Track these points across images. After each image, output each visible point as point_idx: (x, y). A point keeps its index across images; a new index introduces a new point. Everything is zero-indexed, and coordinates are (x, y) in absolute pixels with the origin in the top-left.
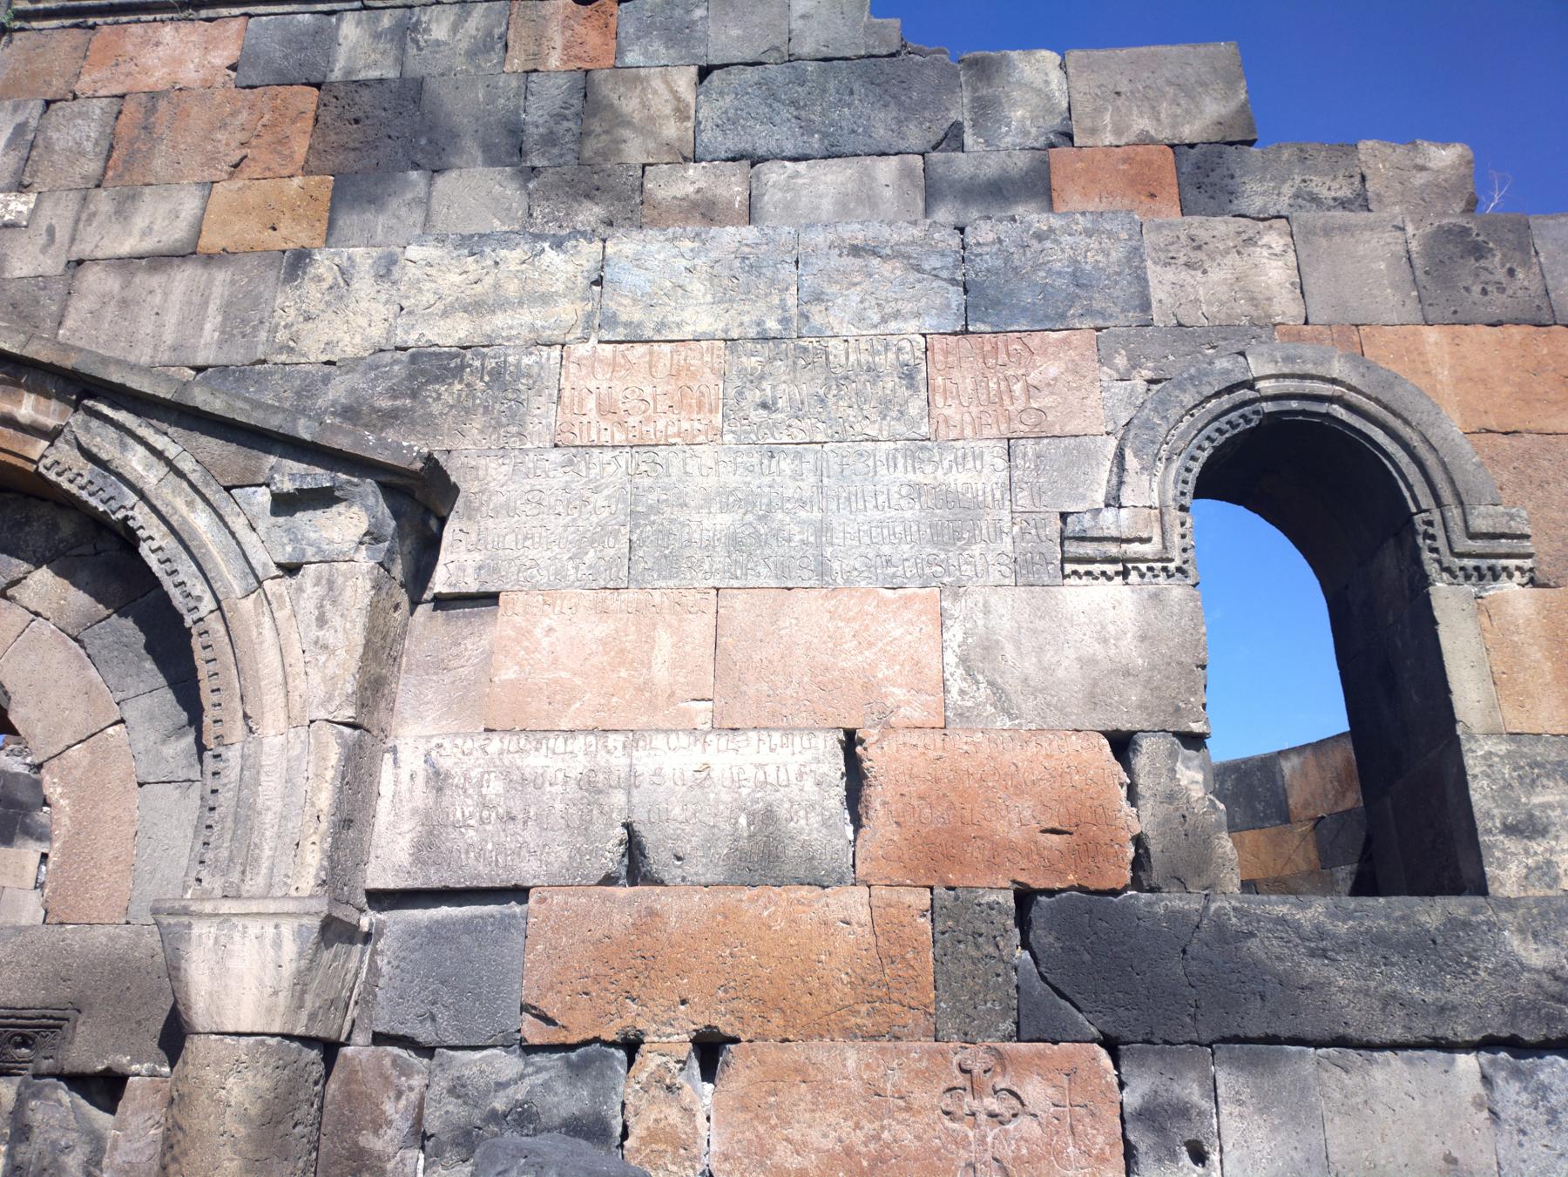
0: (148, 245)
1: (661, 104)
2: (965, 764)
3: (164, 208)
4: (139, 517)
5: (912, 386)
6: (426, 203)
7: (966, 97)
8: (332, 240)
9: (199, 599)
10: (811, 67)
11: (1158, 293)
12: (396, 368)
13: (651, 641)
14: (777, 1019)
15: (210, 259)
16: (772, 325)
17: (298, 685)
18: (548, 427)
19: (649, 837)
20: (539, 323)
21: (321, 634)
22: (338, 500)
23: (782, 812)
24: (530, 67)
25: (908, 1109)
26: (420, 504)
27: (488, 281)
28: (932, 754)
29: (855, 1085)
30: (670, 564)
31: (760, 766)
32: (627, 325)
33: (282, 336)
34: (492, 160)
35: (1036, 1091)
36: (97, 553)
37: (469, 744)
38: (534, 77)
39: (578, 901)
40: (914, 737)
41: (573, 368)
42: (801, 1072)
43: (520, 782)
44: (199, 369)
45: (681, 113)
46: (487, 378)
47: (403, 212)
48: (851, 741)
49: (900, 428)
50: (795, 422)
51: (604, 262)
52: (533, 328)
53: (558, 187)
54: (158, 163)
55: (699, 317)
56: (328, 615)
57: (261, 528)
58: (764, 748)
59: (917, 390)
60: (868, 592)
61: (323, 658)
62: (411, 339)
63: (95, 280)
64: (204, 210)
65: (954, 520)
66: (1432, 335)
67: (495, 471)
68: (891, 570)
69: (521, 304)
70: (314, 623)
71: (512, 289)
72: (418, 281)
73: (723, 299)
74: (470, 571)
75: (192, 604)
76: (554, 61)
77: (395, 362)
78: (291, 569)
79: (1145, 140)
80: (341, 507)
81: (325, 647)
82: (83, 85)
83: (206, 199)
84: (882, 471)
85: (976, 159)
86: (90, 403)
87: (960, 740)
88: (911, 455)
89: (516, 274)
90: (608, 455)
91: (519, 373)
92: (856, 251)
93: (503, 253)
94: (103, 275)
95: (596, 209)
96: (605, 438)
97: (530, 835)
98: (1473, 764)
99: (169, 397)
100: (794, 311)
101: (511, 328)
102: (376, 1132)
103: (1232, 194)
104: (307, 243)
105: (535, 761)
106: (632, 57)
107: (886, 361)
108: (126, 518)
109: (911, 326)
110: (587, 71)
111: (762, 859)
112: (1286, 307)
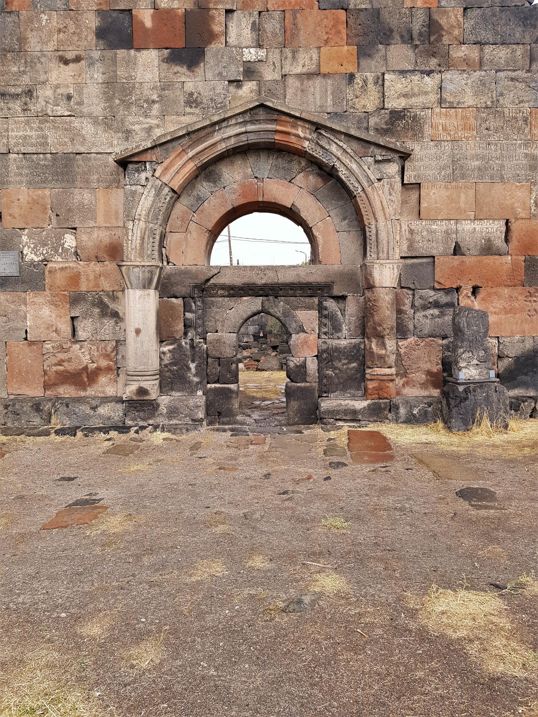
0: (305, 70)
2: (534, 227)
5: (526, 124)
8: (359, 70)
9: (357, 188)
10: (498, 9)
13: (459, 196)
14: (490, 283)
16: (489, 103)
17: (387, 211)
18: (429, 135)
19: (462, 245)
20: (425, 101)
22: (391, 161)
23: (492, 239)
24: (412, 6)
25: (517, 300)
27: (409, 86)
28: (527, 225)
29: (507, 296)
30: (463, 176)
31: (487, 228)
32: (449, 102)
34: (404, 42)
38: (413, 10)
39: (446, 259)
40: (523, 221)
41: (435, 116)
42: (495, 293)
43: (431, 232)
44: (328, 113)
47: (379, 60)
49: (523, 137)
50: (495, 134)
52: (423, 104)
53: (424, 52)
54: (301, 38)
55: (469, 100)
57: (371, 169)
58: (488, 224)
59: (527, 125)
60: (513, 184)
64: (319, 57)
68: (519, 178)
71: (416, 89)
75: (356, 189)
77: (386, 113)
78: (379, 180)
80: (392, 164)
82: (270, 6)
83: (319, 53)
84: (518, 149)
86: (320, 131)
88: (525, 145)
90: (446, 143)
92: (512, 79)
93: (413, 77)
96: (445, 138)
97: (434, 244)
100: (495, 99)
105: (433, 227)
108: (334, 165)
109: (527, 105)
110: (429, 8)
111: (488, 249)
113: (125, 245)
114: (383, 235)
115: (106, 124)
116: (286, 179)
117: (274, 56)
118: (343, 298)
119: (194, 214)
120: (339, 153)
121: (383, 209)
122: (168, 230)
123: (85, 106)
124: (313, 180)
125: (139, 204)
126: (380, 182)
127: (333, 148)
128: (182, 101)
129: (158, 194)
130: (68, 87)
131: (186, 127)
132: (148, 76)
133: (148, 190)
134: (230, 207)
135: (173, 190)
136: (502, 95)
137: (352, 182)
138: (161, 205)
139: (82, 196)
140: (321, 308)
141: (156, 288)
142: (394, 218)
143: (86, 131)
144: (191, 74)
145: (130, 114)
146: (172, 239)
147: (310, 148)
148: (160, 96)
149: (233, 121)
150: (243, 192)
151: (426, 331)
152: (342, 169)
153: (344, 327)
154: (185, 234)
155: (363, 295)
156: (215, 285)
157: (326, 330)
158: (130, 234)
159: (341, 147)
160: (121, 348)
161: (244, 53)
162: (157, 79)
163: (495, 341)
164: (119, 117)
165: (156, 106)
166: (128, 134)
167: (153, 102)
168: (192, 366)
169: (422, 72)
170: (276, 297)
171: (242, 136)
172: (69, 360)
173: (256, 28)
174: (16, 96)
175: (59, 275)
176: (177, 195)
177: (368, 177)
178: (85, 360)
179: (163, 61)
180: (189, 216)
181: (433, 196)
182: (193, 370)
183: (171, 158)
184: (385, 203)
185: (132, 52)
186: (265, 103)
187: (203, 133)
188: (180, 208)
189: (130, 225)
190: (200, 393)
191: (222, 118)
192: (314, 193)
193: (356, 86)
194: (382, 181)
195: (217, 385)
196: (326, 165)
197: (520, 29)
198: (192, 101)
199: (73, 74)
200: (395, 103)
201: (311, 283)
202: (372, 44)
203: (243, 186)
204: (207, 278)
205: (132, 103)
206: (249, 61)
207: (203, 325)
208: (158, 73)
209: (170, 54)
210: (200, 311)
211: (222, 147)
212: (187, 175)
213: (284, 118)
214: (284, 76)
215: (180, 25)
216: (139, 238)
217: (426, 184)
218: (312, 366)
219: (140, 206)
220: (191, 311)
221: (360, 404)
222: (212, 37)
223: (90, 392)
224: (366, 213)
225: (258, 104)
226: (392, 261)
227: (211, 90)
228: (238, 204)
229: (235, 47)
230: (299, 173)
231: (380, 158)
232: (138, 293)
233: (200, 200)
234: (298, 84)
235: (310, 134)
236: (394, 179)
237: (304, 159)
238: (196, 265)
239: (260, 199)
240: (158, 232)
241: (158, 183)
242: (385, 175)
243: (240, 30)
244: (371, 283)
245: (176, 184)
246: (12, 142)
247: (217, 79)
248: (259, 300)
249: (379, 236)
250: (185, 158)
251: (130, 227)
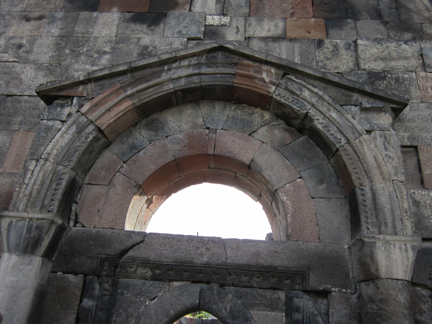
0: (270, 34)
3: (272, 24)
4: (312, 113)
9: (340, 139)
12: (364, 75)
15: (291, 40)
20: (406, 65)
21: (387, 153)
27: (386, 52)
33: (321, 64)
36: (279, 125)
37: (423, 193)
46: (394, 80)
47: (349, 31)
51: (421, 49)
52: (404, 67)
56: (388, 147)
57: (357, 118)
61: (390, 161)
62: (367, 67)
64: (286, 25)
69: (399, 59)
70: (384, 149)
71: (394, 54)
72: (364, 50)
74: (406, 139)
75: (338, 141)
77: (362, 74)
78: (369, 132)
80: (383, 114)
81: (390, 157)
83: (285, 22)
86: (289, 76)
89: (395, 51)
93: (389, 44)
94: (258, 42)
95: (409, 34)
99: (320, 76)
101: (398, 66)
102: (421, 314)
104: (321, 37)
108: (307, 113)
113: (17, 189)
114: (384, 200)
115: (48, 70)
116: (244, 132)
118: (325, 294)
119: (125, 165)
121: (379, 166)
122: (86, 181)
123: (32, 54)
124: (279, 133)
125: (51, 142)
126: (371, 135)
127: (306, 94)
128: (136, 53)
129: (79, 131)
130: (22, 38)
131: (130, 63)
132: (105, 32)
133: (67, 126)
134: (170, 158)
135: (99, 129)
137: (332, 132)
138: (79, 144)
141: (47, 255)
142: (396, 178)
143: (26, 75)
144: (149, 32)
145: (77, 62)
146: (89, 193)
147: (277, 93)
148: (112, 48)
149: (185, 63)
150: (189, 143)
152: (319, 117)
154: (107, 188)
155: (355, 292)
156: (134, 259)
158: (29, 176)
159: (316, 93)
161: (207, 19)
162: (114, 35)
164: (64, 63)
165: (107, 56)
167: (105, 53)
170: (222, 286)
171: (194, 78)
177: (353, 127)
179: (124, 21)
180: (117, 167)
183: (105, 94)
184: (380, 158)
185: (95, 14)
186: (224, 45)
187: (148, 71)
188: (108, 156)
189: (32, 165)
191: (172, 56)
192: (280, 148)
193: (325, 50)
194: (373, 134)
196: (296, 115)
199: (31, 29)
201: (275, 268)
204: (123, 247)
205: (82, 53)
206: (212, 25)
208: (116, 30)
209: (133, 16)
210: (107, 297)
212: (121, 114)
213: (246, 62)
216: (38, 183)
217: (425, 148)
219: (52, 144)
220: (92, 297)
224: (355, 171)
225: (216, 45)
226: (404, 238)
227: (168, 45)
228: (181, 156)
230: (262, 126)
231: (368, 106)
232: (14, 258)
233: (135, 149)
234: (262, 45)
235: (277, 79)
236: (388, 132)
237: (267, 112)
238: (112, 229)
239: (211, 152)
241: (83, 119)
242: (375, 127)
244: (373, 270)
247: (176, 36)
248: (197, 288)
249: (378, 201)
250: (123, 96)
251: (32, 168)
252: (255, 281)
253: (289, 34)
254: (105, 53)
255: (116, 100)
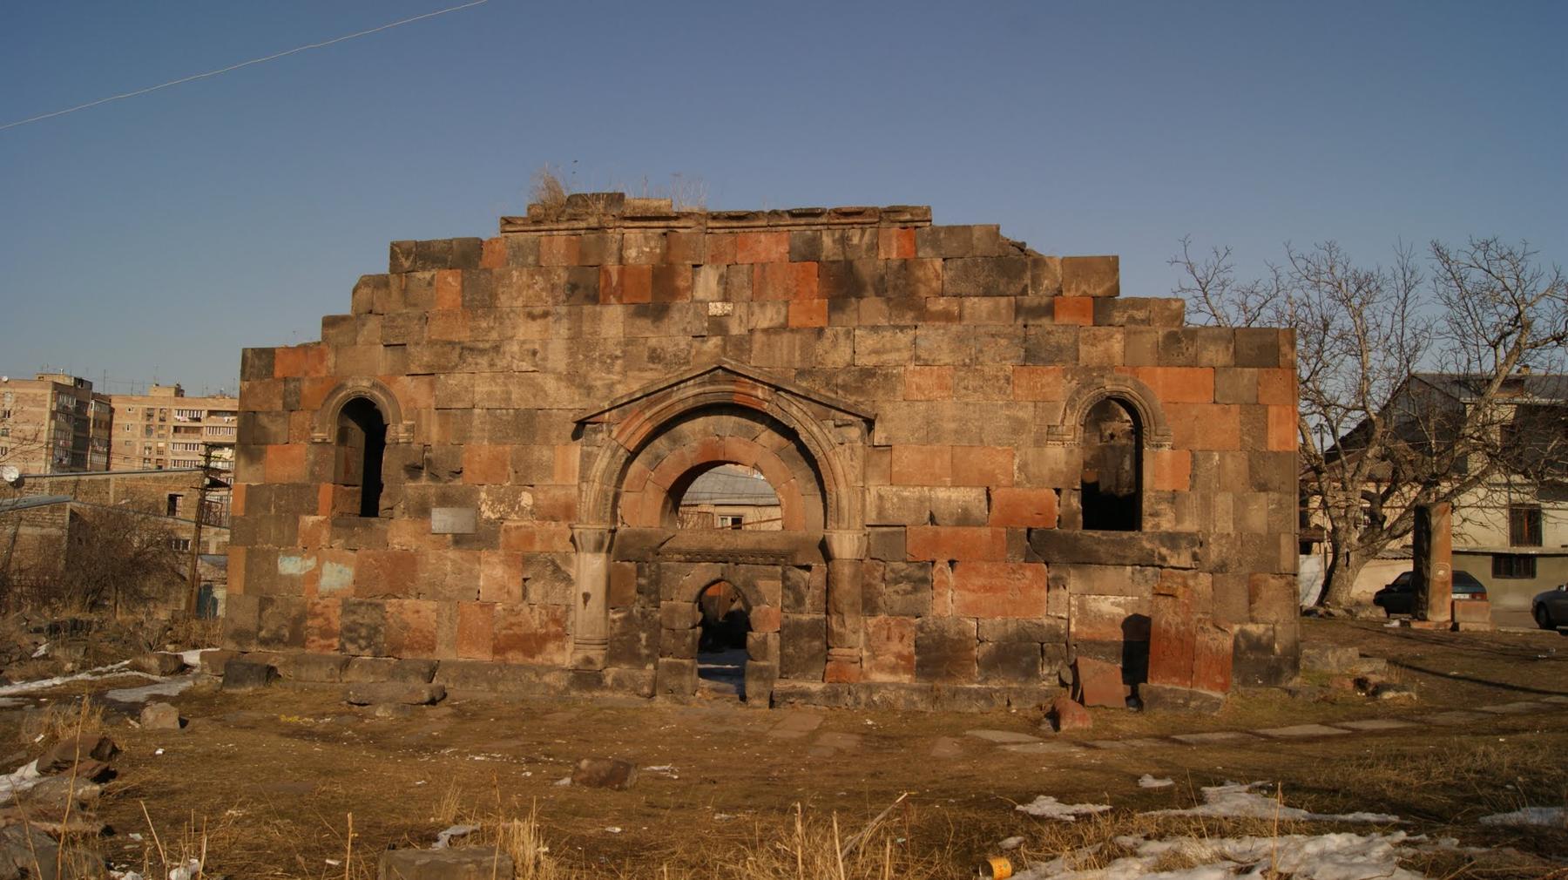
1: (931, 275)
6: (858, 309)
7: (1029, 274)
11: (1082, 354)
15: (792, 331)
26: (870, 424)
30: (938, 439)
34: (878, 295)
35: (1028, 574)
43: (903, 499)
45: (937, 276)
48: (988, 490)
54: (770, 292)
63: (758, 337)
65: (1018, 427)
66: (1159, 370)
67: (888, 407)
71: (888, 346)
73: (952, 351)
76: (894, 255)
79: (1085, 294)
85: (1031, 299)
87: (1017, 490)
91: (893, 375)
98: (1145, 499)
103: (1110, 316)
106: (921, 254)
107: (1001, 374)
111: (964, 519)
112: (1118, 361)
117: (742, 310)
120: (800, 415)
127: (794, 410)
129: (613, 456)
134: (688, 466)
136: (981, 351)
139: (542, 453)
140: (785, 578)
141: (609, 551)
151: (897, 609)
153: (808, 601)
156: (670, 550)
157: (787, 602)
160: (572, 614)
163: (974, 624)
165: (619, 362)
166: (589, 390)
167: (617, 357)
168: (643, 636)
169: (896, 327)
172: (519, 624)
173: (724, 281)
174: (483, 352)
175: (513, 534)
176: (633, 455)
178: (535, 623)
181: (907, 457)
182: (644, 642)
185: (598, 308)
190: (650, 667)
192: (779, 452)
195: (670, 659)
197: (1004, 281)
198: (655, 357)
200: (865, 361)
202: (846, 296)
203: (705, 445)
207: (657, 592)
211: (680, 408)
214: (751, 331)
215: (647, 280)
218: (774, 641)
221: (816, 687)
222: (675, 293)
223: (539, 659)
229: (701, 302)
233: (659, 458)
234: (764, 338)
240: (611, 494)
243: (707, 282)
245: (632, 445)
246: (477, 397)
252: (760, 560)
253: (793, 323)
254: (617, 357)
255: (637, 423)
